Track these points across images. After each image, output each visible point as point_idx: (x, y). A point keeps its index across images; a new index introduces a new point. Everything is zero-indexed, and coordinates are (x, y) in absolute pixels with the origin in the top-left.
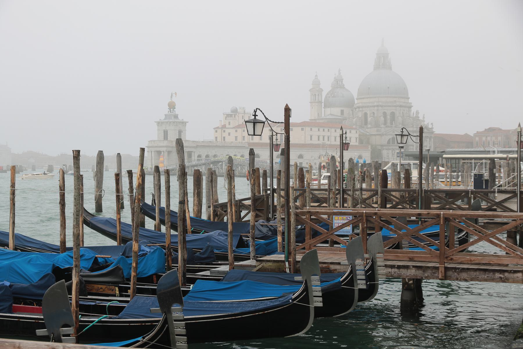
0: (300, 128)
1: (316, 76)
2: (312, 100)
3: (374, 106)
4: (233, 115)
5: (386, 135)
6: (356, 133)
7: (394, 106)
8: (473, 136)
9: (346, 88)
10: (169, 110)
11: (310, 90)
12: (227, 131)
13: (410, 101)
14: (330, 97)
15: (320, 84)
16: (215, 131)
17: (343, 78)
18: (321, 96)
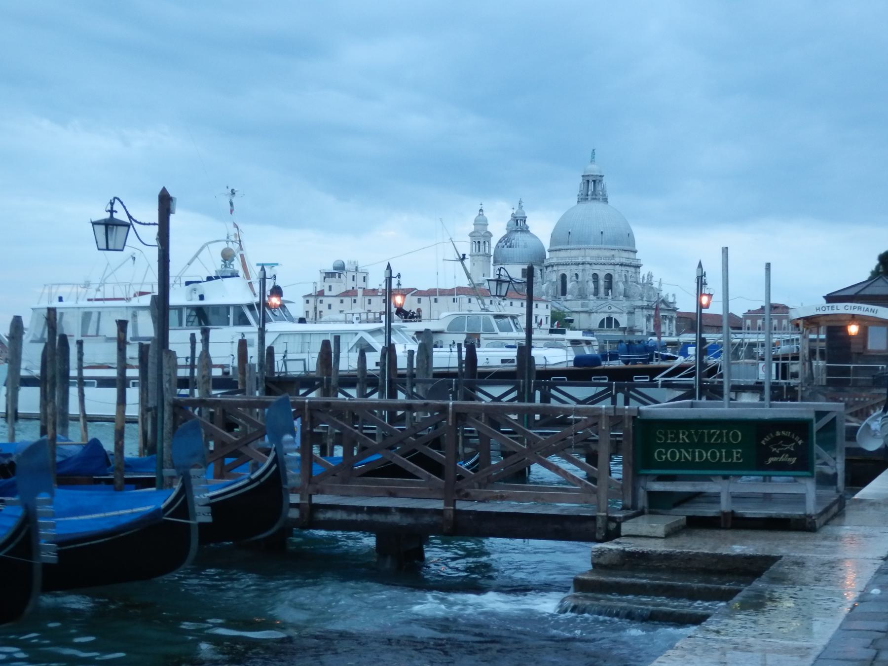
0: (451, 298)
1: (481, 210)
2: (474, 251)
4: (337, 275)
5: (597, 313)
6: (547, 308)
7: (611, 264)
8: (741, 317)
9: (531, 232)
10: (223, 263)
11: (471, 235)
12: (326, 301)
13: (638, 256)
14: (503, 247)
15: (488, 225)
16: (305, 302)
17: (526, 215)
18: (489, 244)
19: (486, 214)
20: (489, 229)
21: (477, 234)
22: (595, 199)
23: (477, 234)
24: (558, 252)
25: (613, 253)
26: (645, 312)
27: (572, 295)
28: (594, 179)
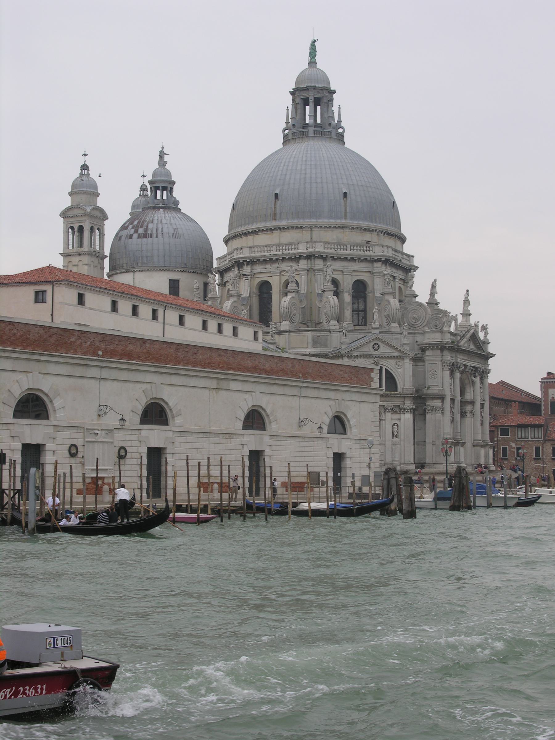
0: (29, 292)
1: (85, 167)
2: (70, 248)
3: (297, 258)
7: (366, 260)
11: (64, 214)
14: (131, 237)
15: (98, 195)
18: (102, 235)
19: (93, 174)
20: (101, 202)
21: (76, 212)
22: (321, 133)
23: (76, 212)
24: (250, 237)
25: (368, 237)
26: (448, 357)
27: (291, 321)
28: (318, 96)
